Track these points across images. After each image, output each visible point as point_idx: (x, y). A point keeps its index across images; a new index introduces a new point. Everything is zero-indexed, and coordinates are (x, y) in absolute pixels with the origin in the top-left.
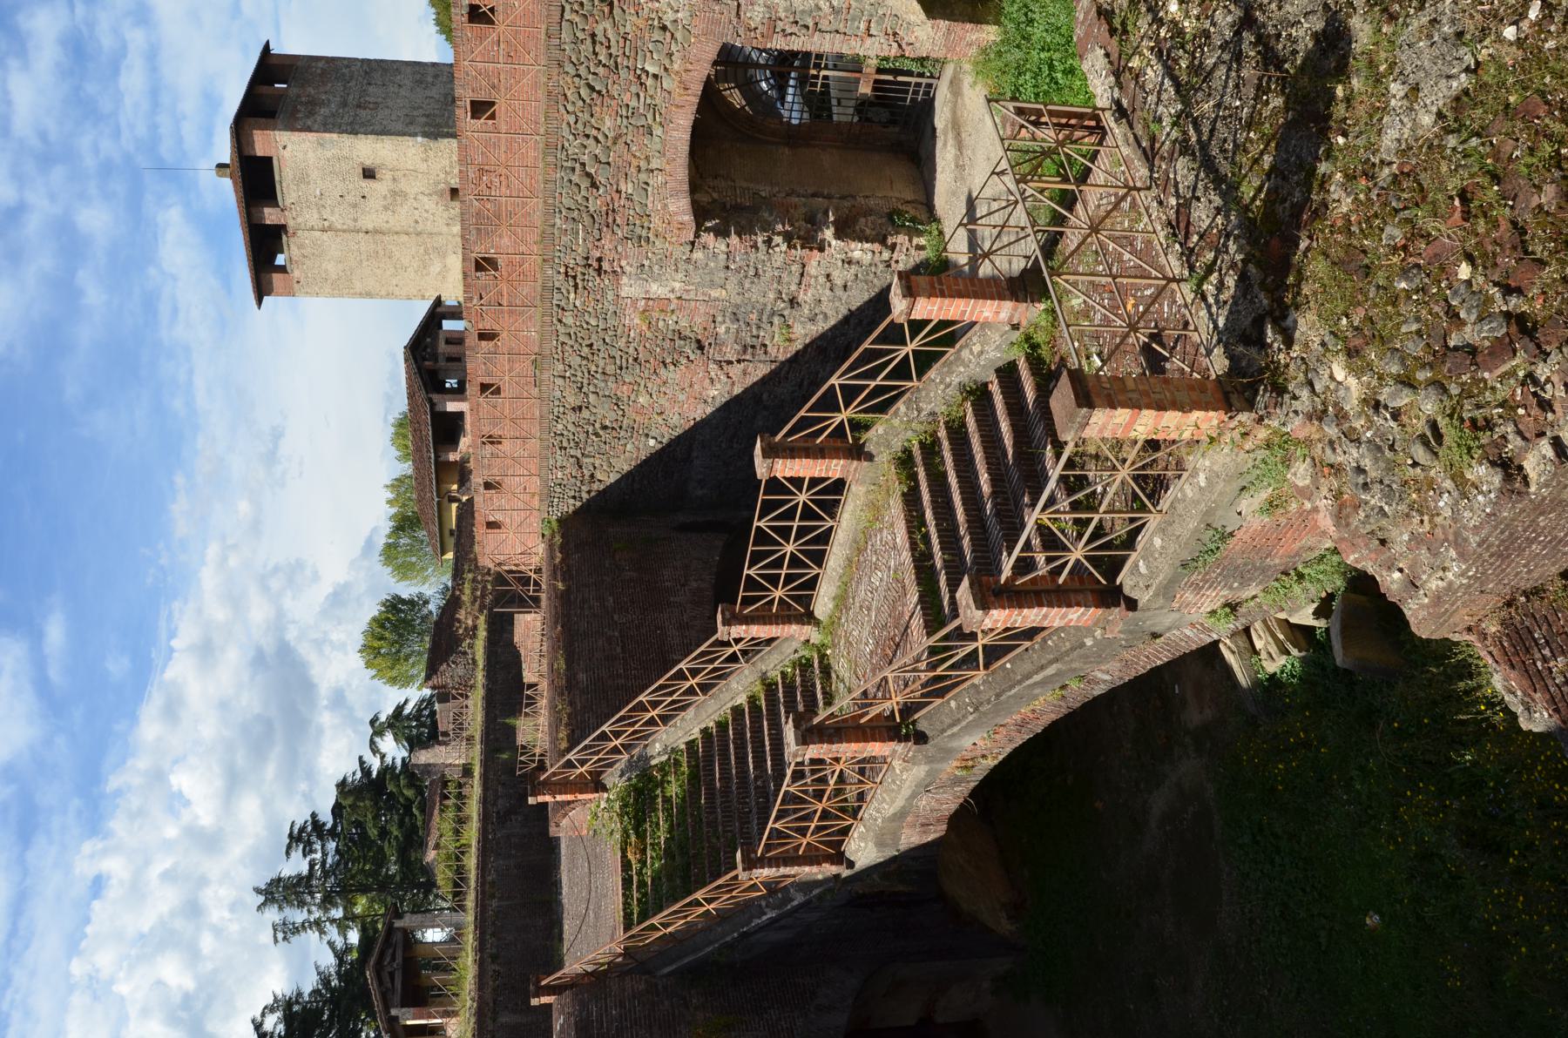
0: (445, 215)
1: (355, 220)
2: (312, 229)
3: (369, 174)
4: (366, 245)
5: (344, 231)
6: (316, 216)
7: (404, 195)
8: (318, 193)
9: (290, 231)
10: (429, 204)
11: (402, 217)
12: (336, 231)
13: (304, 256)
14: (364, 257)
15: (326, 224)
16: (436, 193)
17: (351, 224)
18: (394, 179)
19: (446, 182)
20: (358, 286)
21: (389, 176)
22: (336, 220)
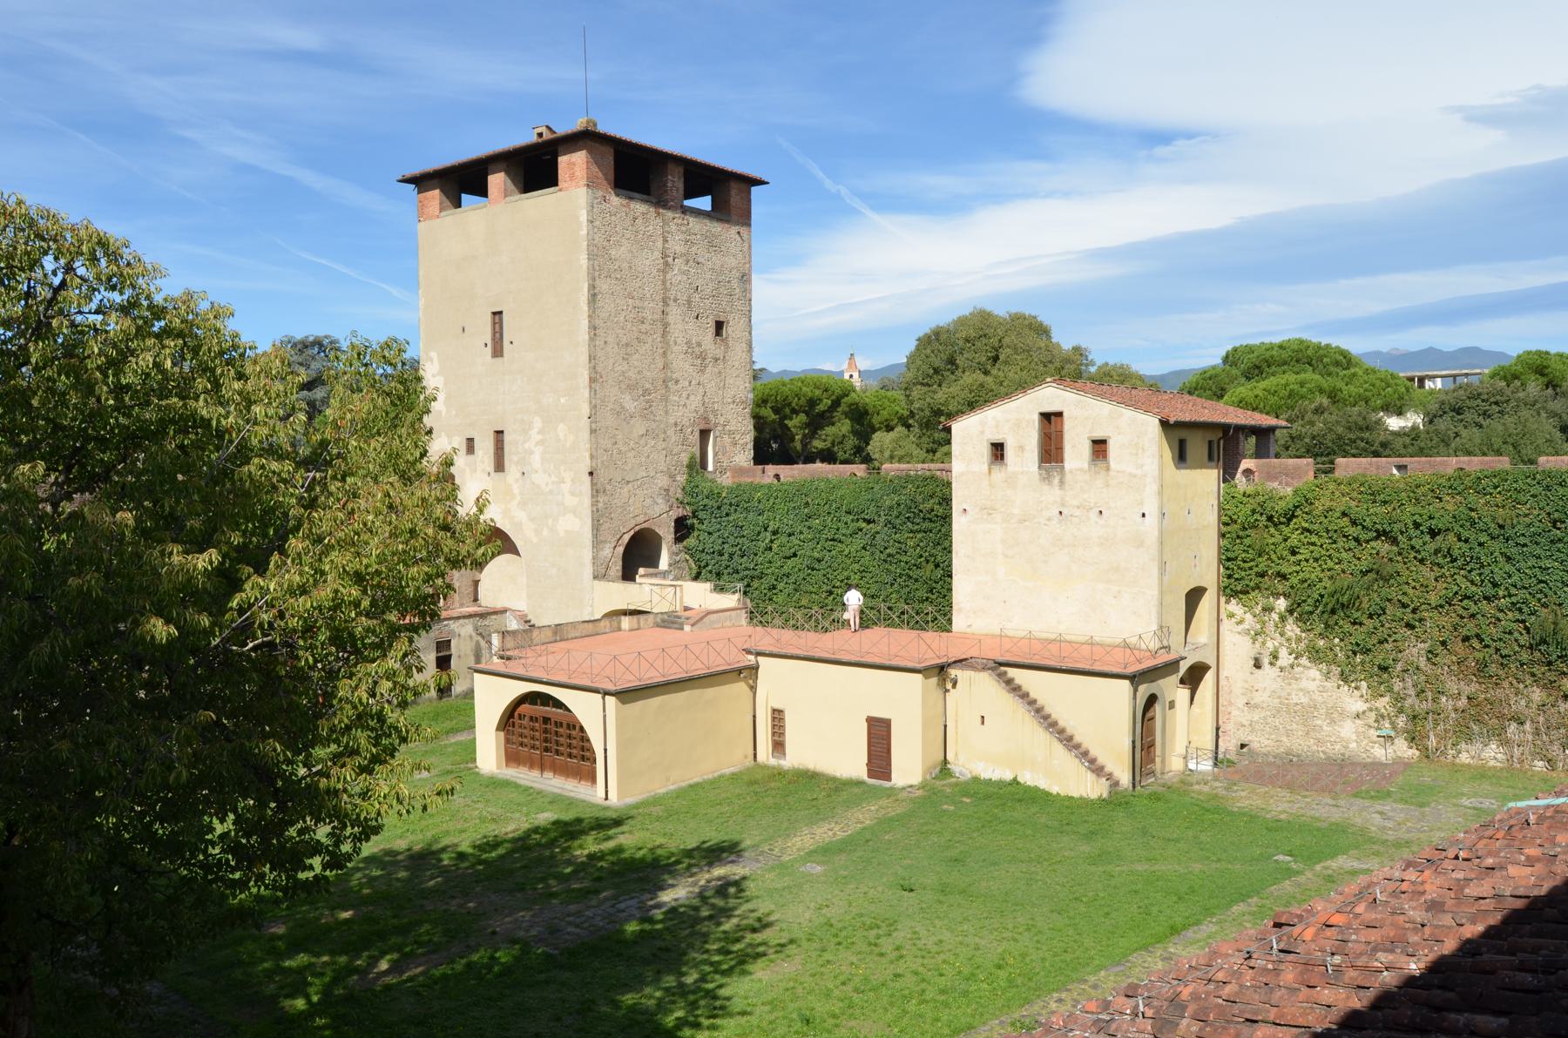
0: (685, 422)
1: (675, 300)
2: (665, 241)
3: (719, 326)
4: (651, 309)
5: (664, 282)
6: (679, 248)
7: (702, 371)
8: (700, 260)
9: (661, 211)
10: (695, 402)
11: (682, 366)
12: (664, 272)
13: (635, 219)
14: (638, 303)
15: (670, 260)
16: (705, 411)
17: (672, 294)
18: (717, 360)
19: (716, 425)
20: (603, 285)
21: (719, 352)
22: (675, 275)
